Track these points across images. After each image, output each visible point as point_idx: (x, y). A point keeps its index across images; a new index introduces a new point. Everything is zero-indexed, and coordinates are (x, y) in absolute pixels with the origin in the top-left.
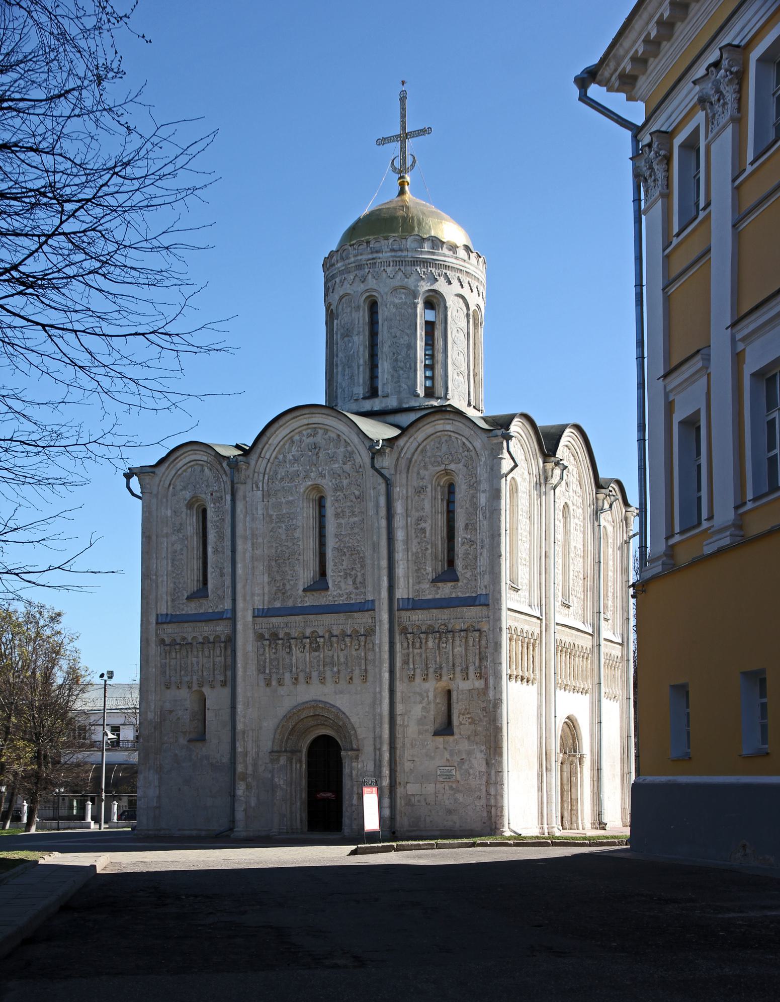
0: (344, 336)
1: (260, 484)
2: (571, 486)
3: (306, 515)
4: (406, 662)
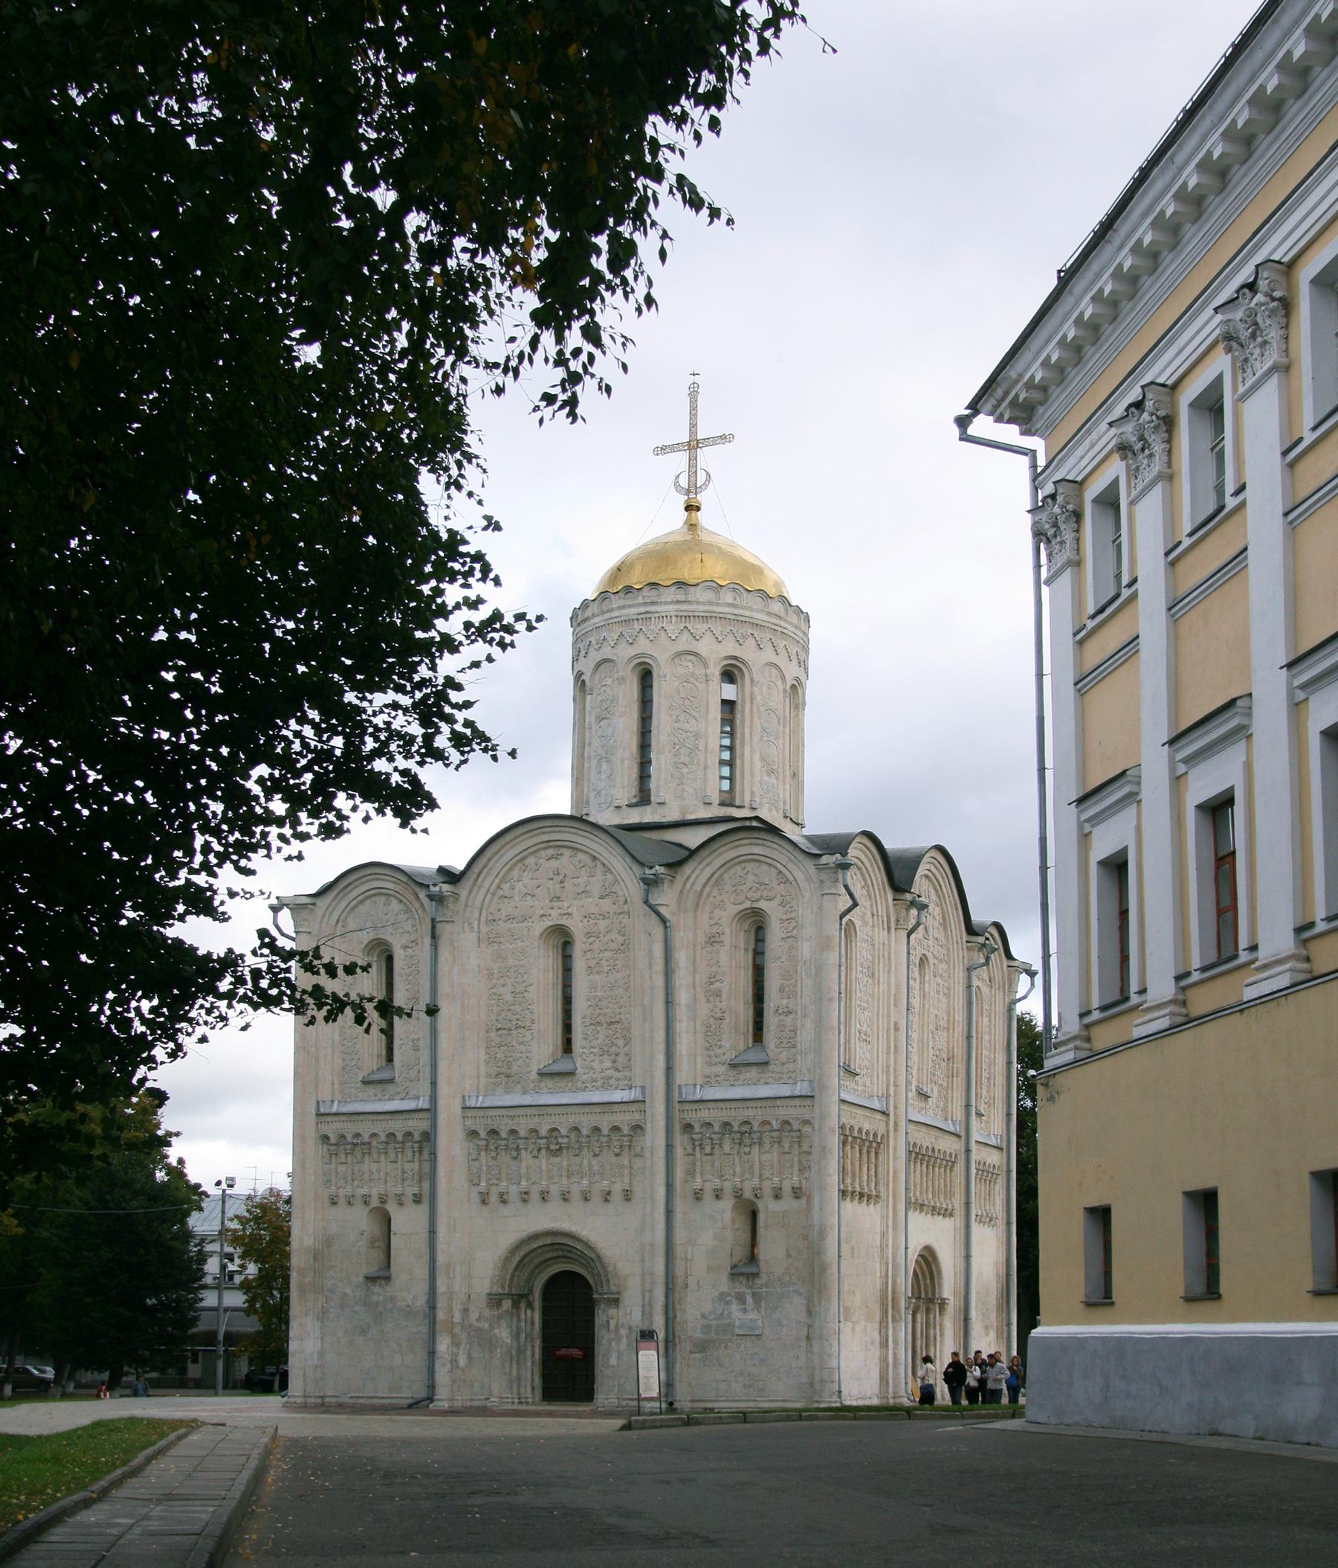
0: (600, 719)
2: (931, 931)
3: (543, 966)
4: (690, 1173)
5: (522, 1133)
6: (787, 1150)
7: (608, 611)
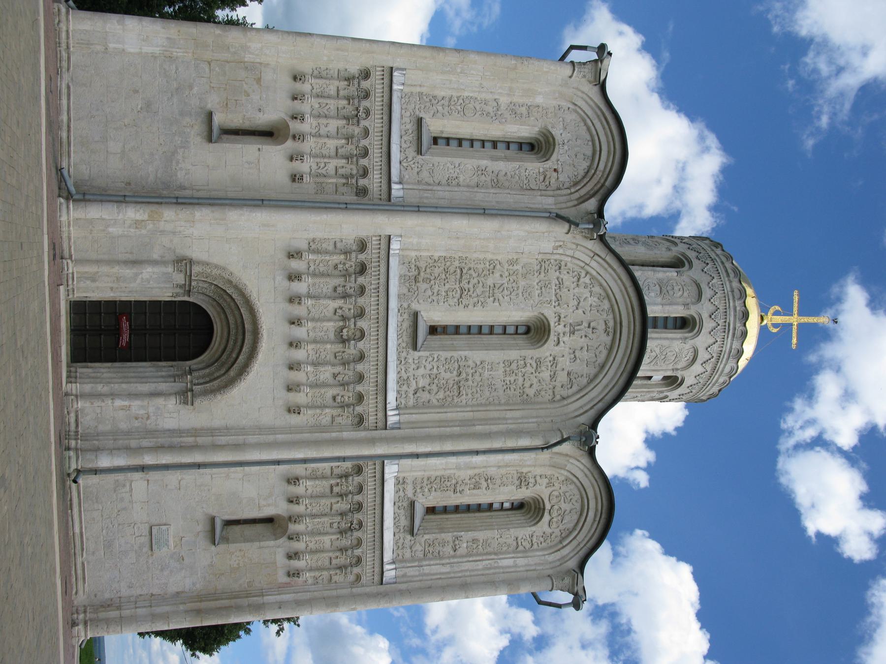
1: (561, 251)
5: (361, 301)
7: (734, 297)
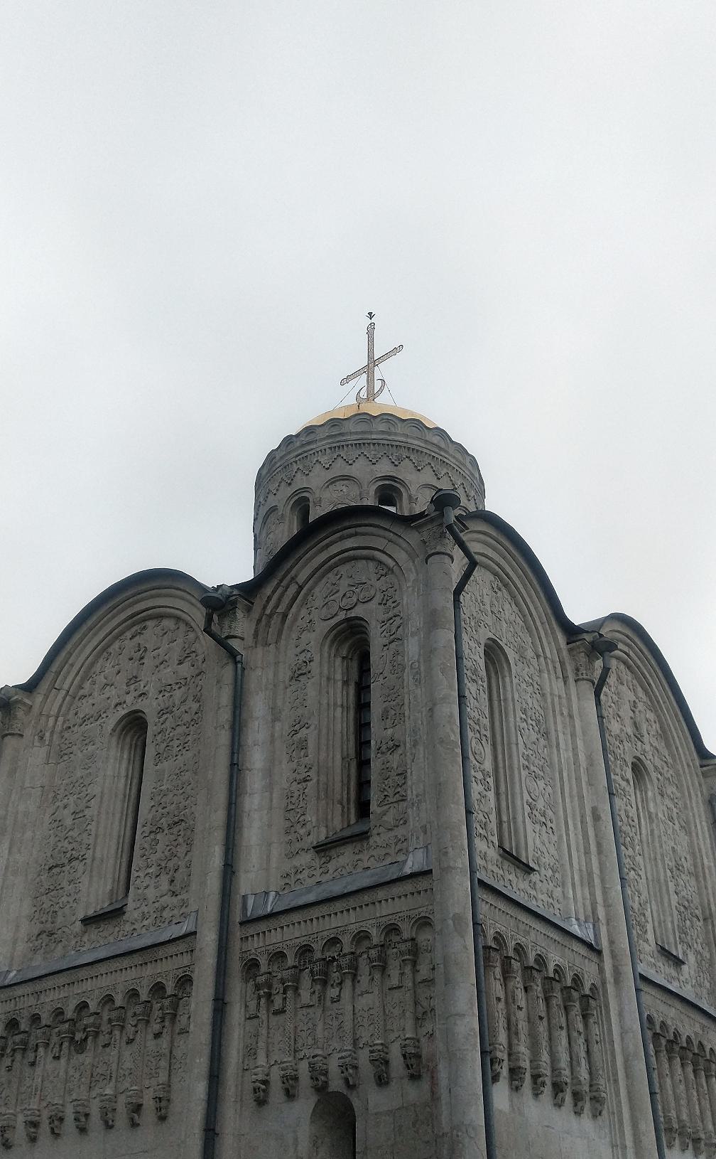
4: (251, 1052)
6: (395, 981)
